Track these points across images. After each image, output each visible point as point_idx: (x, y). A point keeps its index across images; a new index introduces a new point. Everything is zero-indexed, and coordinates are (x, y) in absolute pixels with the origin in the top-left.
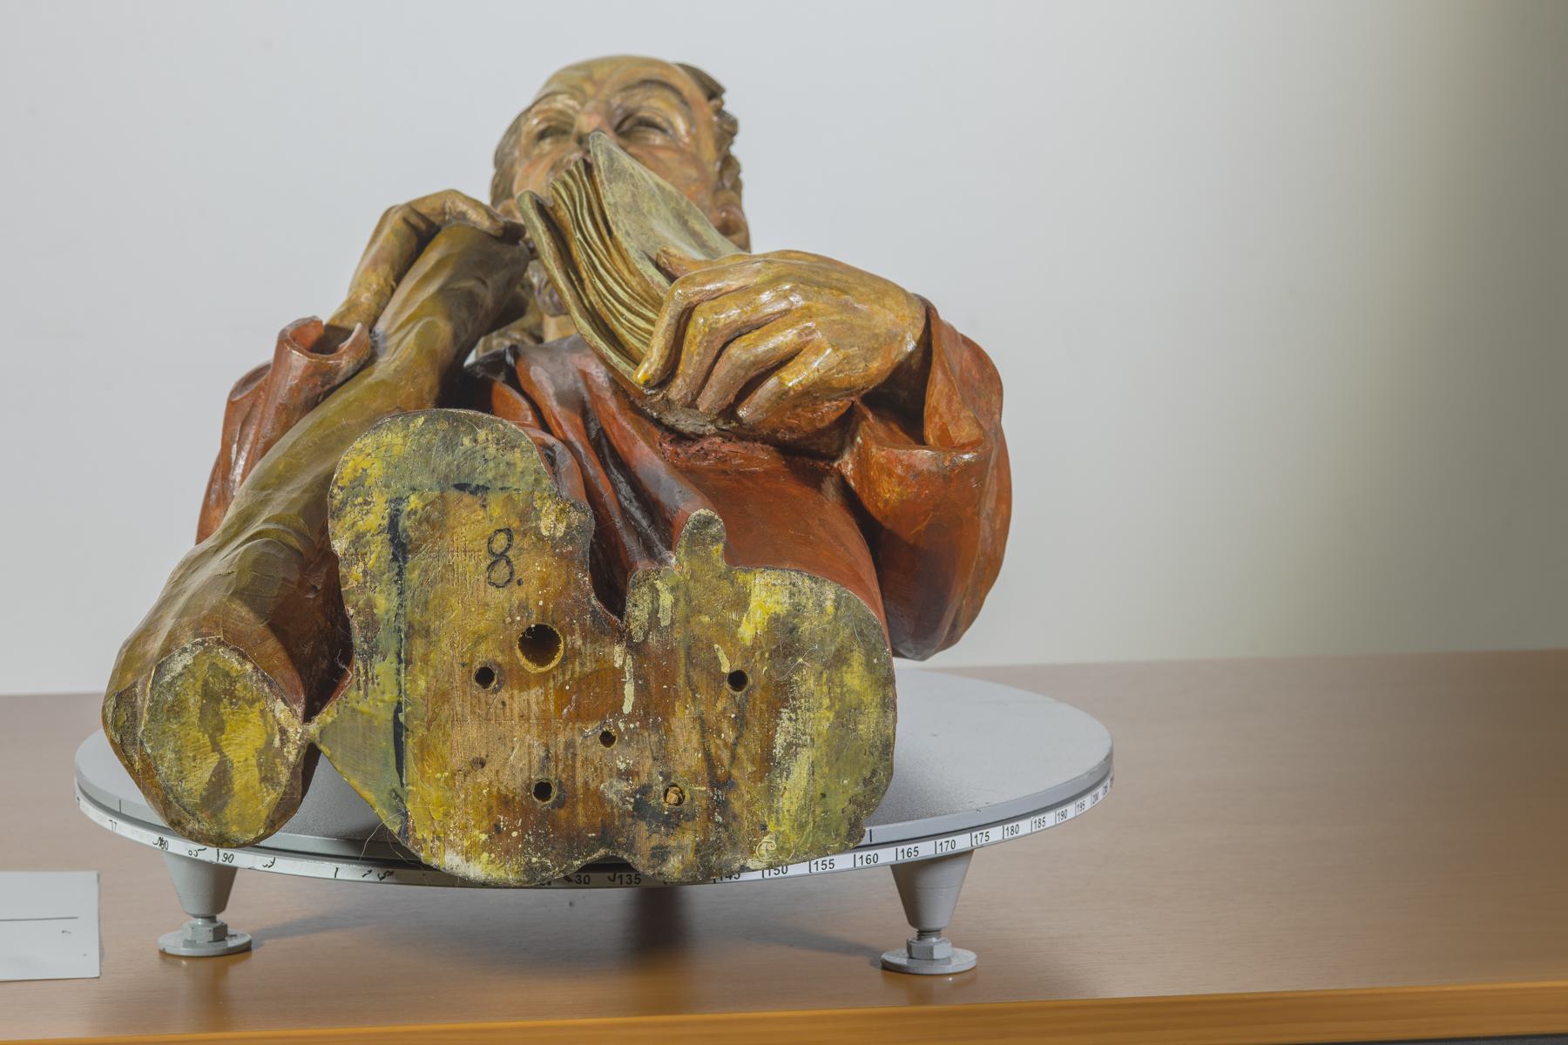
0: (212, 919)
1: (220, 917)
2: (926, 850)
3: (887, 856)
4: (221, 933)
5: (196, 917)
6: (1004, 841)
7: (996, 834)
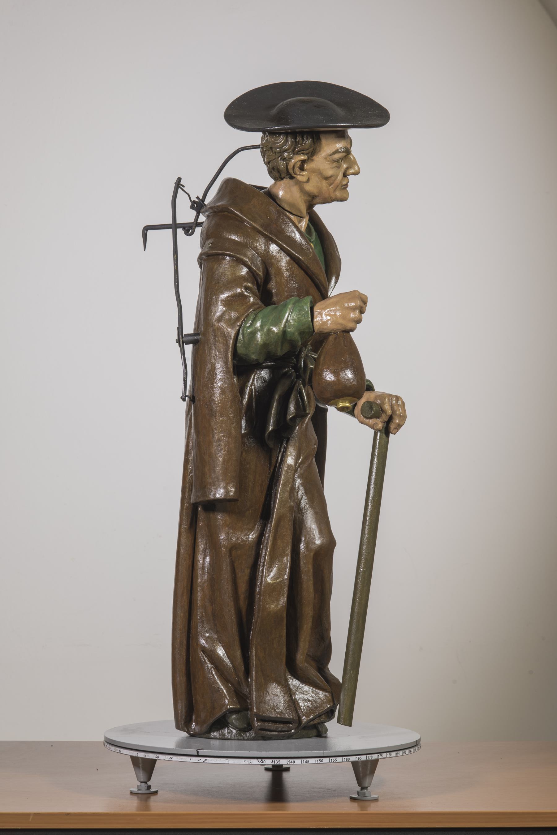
0: (146, 783)
1: (149, 783)
2: (364, 758)
3: (352, 759)
4: (149, 787)
5: (141, 782)
6: (387, 758)
7: (384, 755)
